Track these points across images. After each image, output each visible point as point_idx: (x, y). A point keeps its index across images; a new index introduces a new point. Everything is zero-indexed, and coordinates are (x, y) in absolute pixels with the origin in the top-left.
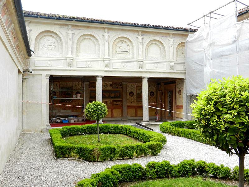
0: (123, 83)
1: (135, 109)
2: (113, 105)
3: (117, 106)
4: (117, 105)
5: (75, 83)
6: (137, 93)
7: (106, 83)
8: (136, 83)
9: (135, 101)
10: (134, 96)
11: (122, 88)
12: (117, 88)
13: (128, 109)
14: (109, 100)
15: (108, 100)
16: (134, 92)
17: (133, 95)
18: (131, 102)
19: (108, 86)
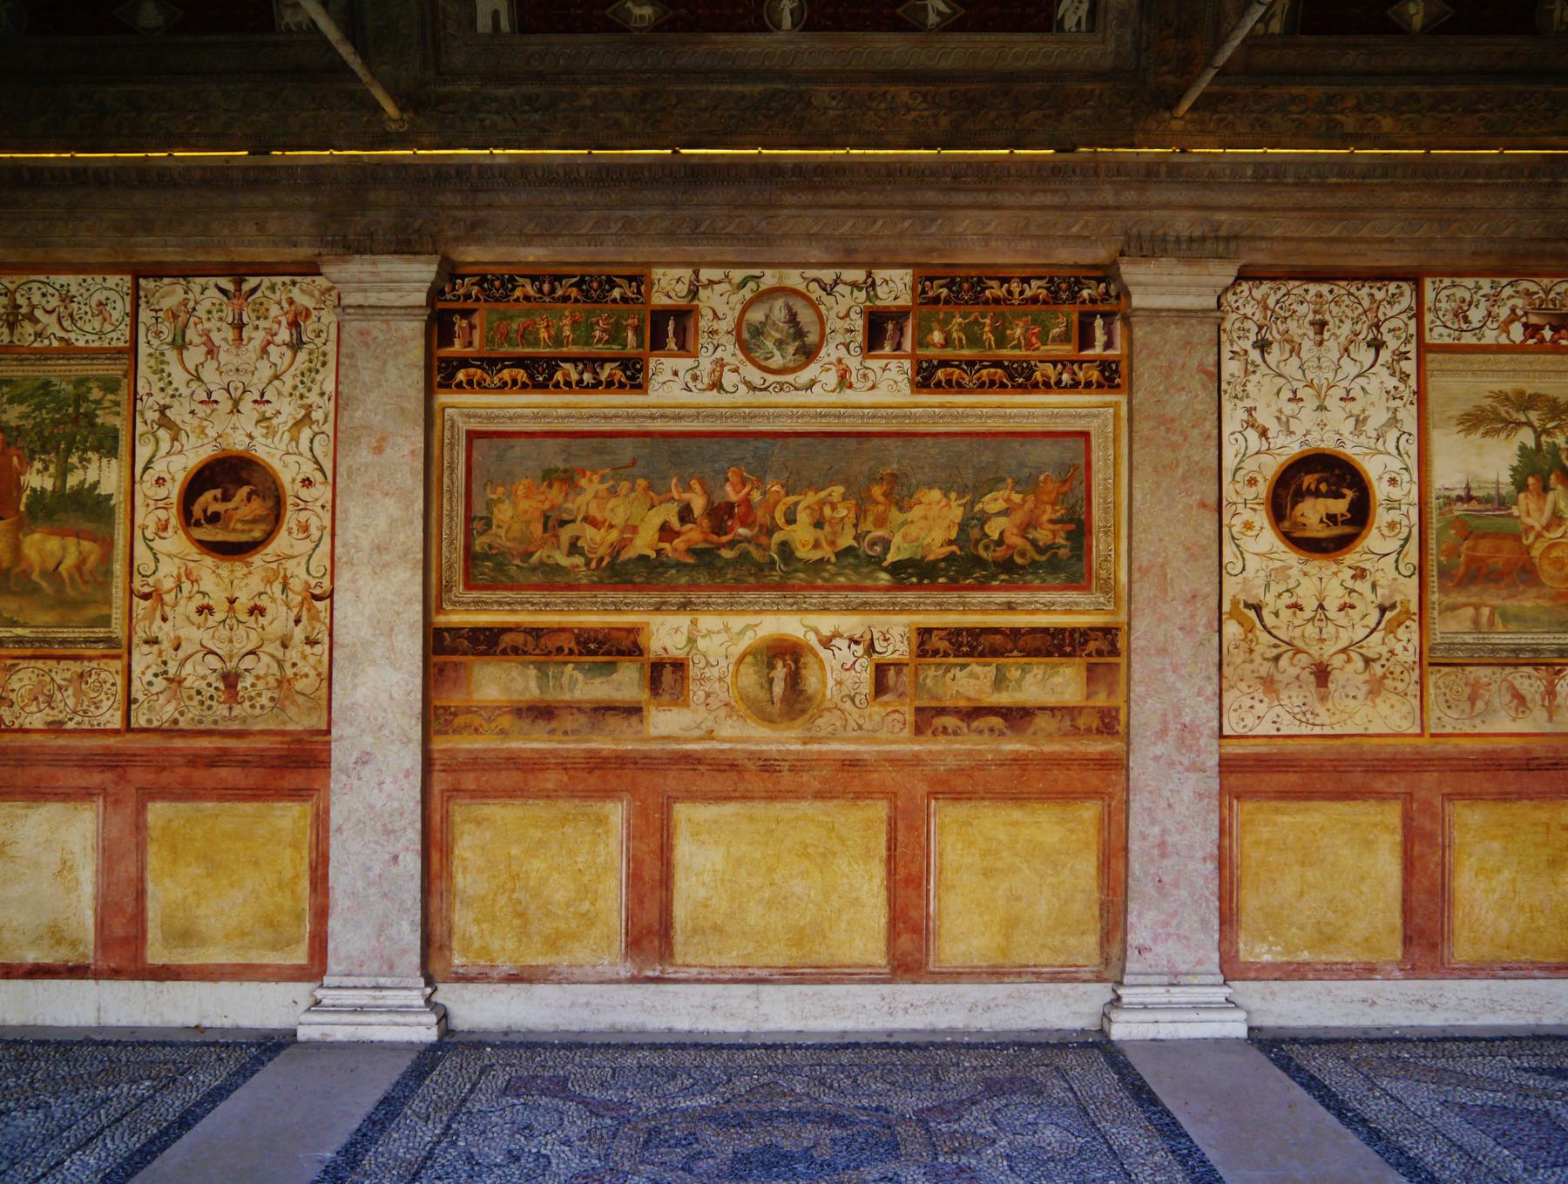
0: (1131, 272)
1: (1392, 814)
2: (926, 719)
3: (1013, 746)
4: (1017, 717)
5: (170, 294)
6: (1448, 476)
7: (793, 278)
8: (1415, 278)
9: (1409, 635)
10: (1374, 540)
11: (1111, 377)
12: (1020, 378)
13: (1244, 810)
14: (851, 623)
15: (827, 623)
16: (1373, 468)
17: (1360, 514)
18: (1322, 674)
19: (830, 352)
